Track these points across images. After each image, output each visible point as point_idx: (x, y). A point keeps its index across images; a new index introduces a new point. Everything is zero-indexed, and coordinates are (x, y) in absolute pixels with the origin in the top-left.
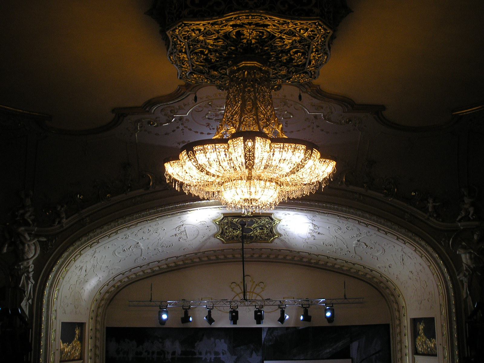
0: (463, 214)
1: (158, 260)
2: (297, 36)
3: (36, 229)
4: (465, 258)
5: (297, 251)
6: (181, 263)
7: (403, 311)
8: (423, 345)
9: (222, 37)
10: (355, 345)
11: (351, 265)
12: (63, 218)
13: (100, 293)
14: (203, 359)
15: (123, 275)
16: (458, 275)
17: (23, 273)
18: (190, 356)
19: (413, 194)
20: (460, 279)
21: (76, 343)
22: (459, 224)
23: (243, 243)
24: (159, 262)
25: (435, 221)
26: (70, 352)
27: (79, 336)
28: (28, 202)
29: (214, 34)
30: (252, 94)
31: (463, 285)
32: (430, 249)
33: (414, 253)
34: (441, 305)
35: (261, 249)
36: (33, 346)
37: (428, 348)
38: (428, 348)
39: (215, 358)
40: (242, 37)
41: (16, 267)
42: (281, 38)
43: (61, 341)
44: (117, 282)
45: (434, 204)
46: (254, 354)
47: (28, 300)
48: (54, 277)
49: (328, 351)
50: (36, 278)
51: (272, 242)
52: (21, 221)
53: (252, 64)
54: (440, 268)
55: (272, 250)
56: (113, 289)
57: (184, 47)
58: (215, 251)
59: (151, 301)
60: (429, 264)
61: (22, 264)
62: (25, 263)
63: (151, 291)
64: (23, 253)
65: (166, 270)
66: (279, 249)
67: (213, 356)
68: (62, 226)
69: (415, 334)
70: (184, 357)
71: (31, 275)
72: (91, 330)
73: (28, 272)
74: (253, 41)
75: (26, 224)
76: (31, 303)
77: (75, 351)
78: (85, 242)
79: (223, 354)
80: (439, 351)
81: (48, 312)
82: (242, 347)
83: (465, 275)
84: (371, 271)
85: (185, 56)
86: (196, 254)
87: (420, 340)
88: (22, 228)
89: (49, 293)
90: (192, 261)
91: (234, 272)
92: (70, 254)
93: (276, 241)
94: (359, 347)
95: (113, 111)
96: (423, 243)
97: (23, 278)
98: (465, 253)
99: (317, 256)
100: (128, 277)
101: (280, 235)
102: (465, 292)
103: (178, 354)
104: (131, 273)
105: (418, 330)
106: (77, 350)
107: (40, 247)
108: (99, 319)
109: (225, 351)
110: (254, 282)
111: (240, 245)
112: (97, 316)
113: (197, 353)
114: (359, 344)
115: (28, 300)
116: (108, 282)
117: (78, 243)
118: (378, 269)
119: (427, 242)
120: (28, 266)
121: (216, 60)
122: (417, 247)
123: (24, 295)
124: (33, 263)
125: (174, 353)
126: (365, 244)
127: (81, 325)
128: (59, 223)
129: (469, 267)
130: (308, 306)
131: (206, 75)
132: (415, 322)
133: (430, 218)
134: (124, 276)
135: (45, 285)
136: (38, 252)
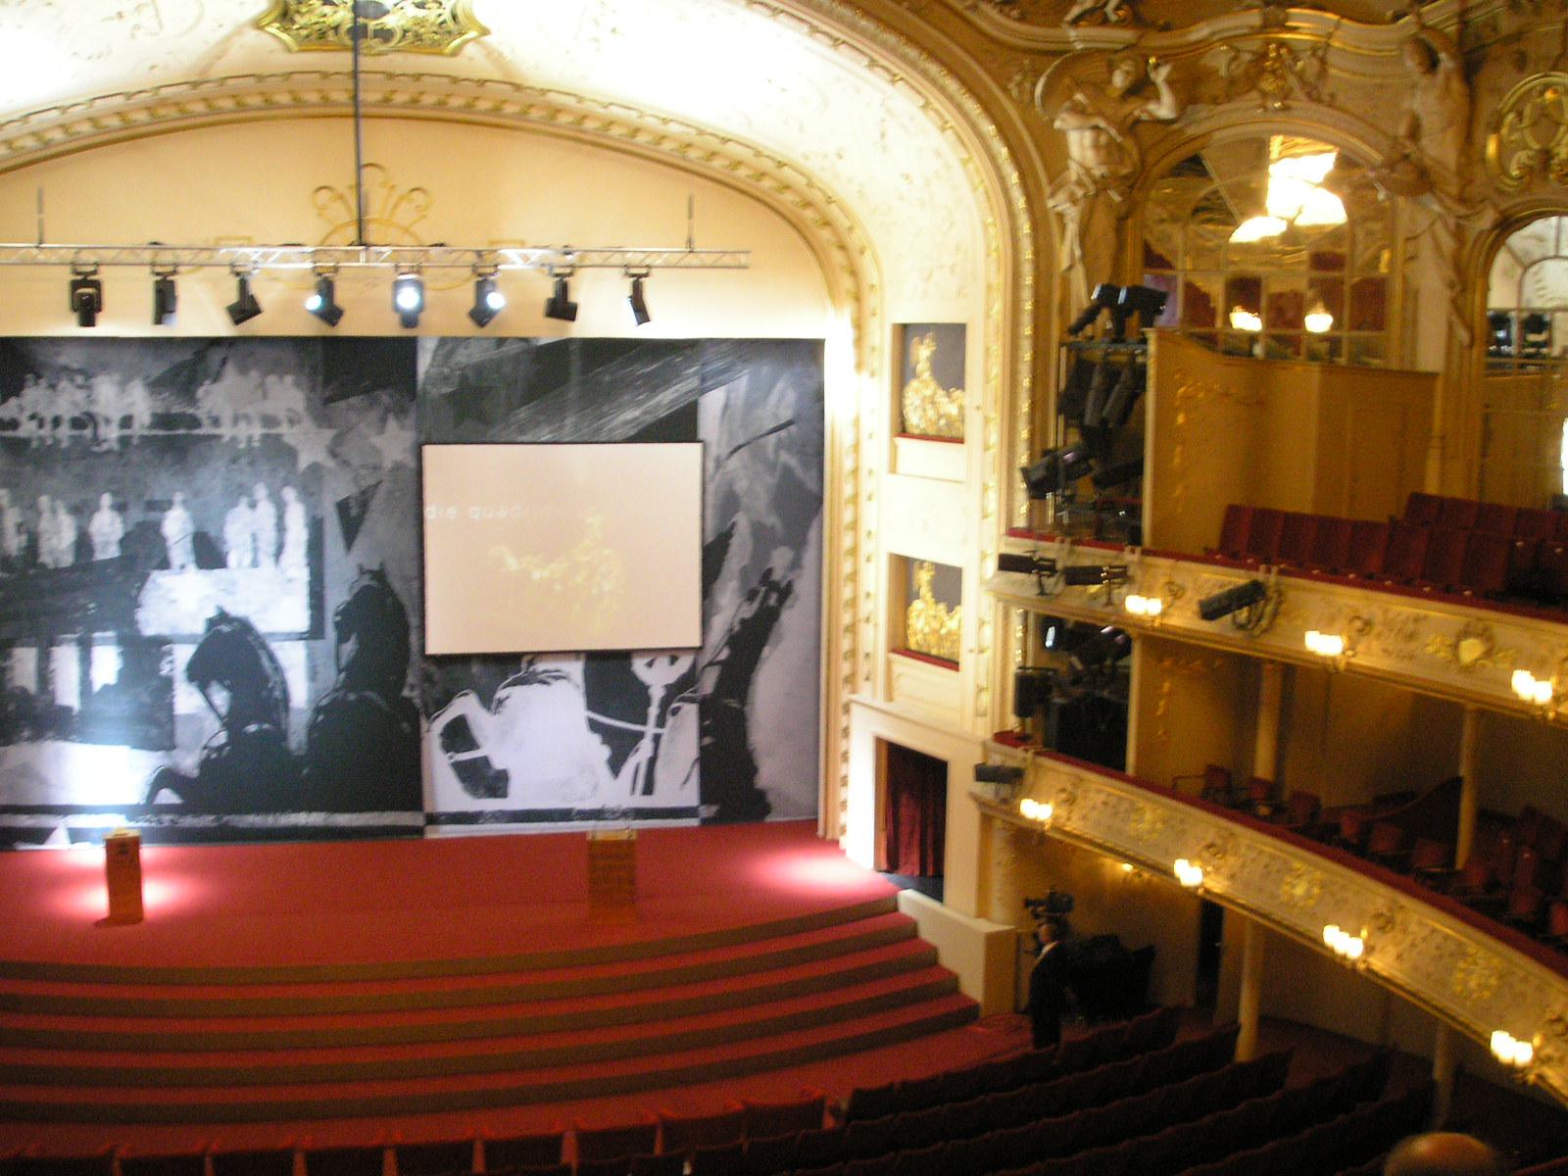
4: (1080, 146)
5: (539, 86)
6: (142, 117)
7: (871, 301)
8: (924, 410)
10: (712, 405)
11: (715, 144)
14: (226, 439)
16: (1053, 195)
18: (182, 432)
20: (1059, 209)
22: (1072, 33)
23: (355, 50)
24: (64, 109)
25: (994, 13)
31: (1063, 228)
32: (972, 107)
33: (920, 115)
34: (989, 287)
35: (418, 77)
37: (940, 417)
38: (940, 417)
39: (265, 437)
46: (392, 424)
49: (630, 414)
51: (455, 53)
54: (997, 169)
55: (455, 80)
58: (260, 78)
60: (965, 156)
63: (41, 211)
65: (91, 141)
66: (478, 81)
67: (257, 431)
69: (903, 373)
70: (161, 433)
79: (292, 422)
80: (973, 430)
82: (353, 400)
83: (1074, 201)
84: (781, 165)
86: (195, 85)
87: (917, 391)
90: (181, 111)
91: (327, 151)
93: (470, 50)
94: (726, 407)
96: (952, 85)
98: (1080, 128)
99: (605, 107)
101: (485, 32)
102: (1067, 250)
105: (913, 359)
109: (297, 413)
110: (393, 187)
111: (343, 61)
113: (206, 422)
114: (728, 399)
118: (801, 162)
119: (963, 82)
122: (932, 100)
125: (127, 422)
129: (1088, 171)
130: (568, 271)
132: (905, 333)
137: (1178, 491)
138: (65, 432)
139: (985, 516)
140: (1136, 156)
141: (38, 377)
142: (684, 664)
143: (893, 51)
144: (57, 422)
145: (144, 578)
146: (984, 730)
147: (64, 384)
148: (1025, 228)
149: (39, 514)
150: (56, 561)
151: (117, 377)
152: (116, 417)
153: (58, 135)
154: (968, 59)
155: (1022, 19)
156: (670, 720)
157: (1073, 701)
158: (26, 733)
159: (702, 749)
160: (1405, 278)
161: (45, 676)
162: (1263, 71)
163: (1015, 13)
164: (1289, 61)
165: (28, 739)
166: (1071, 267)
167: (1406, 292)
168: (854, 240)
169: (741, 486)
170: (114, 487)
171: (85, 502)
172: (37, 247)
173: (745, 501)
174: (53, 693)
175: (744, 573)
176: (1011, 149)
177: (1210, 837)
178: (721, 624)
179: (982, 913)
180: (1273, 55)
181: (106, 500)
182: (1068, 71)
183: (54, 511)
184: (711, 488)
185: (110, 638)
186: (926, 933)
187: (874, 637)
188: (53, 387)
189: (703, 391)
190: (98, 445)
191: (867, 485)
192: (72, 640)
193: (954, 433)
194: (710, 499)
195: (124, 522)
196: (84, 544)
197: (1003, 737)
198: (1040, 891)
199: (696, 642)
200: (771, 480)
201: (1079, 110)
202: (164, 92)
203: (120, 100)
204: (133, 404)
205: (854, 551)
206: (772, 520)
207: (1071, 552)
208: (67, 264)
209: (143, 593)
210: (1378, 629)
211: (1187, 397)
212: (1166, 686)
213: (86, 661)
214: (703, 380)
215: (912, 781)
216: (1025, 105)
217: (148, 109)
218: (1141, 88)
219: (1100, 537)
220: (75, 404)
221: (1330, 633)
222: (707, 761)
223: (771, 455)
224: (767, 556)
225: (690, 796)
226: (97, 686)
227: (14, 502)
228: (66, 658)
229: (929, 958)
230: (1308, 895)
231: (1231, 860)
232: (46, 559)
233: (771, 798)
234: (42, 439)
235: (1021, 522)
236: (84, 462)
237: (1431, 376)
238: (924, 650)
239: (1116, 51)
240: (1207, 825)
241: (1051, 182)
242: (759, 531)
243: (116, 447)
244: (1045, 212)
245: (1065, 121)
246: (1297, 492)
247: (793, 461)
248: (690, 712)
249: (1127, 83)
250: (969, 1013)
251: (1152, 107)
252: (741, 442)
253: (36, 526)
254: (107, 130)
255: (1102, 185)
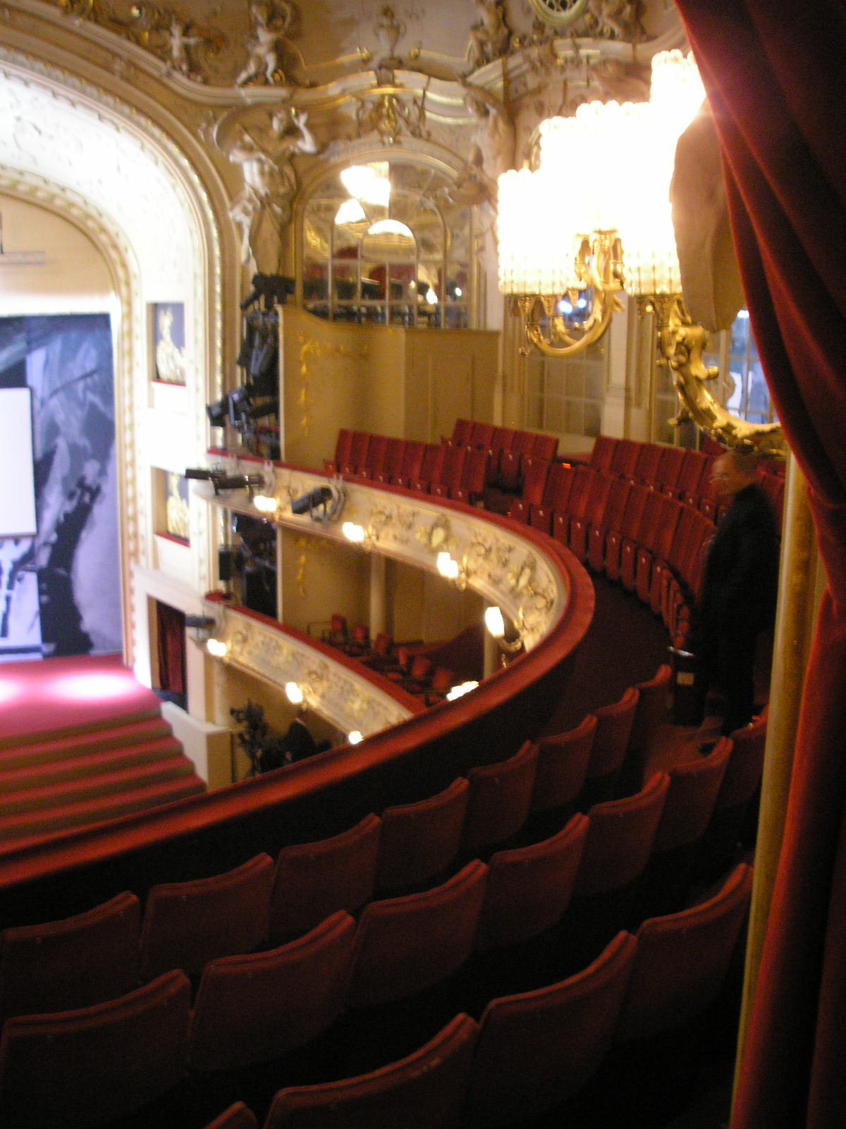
0: (252, 68)
7: (134, 285)
8: (168, 363)
10: (36, 362)
11: (17, 177)
16: (232, 209)
19: (135, 12)
22: (243, 92)
25: (184, 80)
34: (195, 276)
37: (176, 367)
45: (185, 40)
60: (173, 181)
69: (155, 337)
80: (189, 379)
83: (246, 212)
84: (63, 190)
102: (243, 249)
105: (160, 327)
126: (36, 128)
129: (256, 192)
132: (155, 309)
133: (177, 75)
137: (304, 422)
139: (198, 438)
140: (293, 180)
142: (25, 546)
143: (114, 109)
146: (204, 588)
148: (215, 233)
154: (168, 114)
155: (206, 82)
156: (17, 584)
157: (249, 571)
159: (42, 606)
160: (479, 265)
162: (380, 117)
163: (199, 78)
164: (398, 109)
166: (248, 260)
167: (479, 273)
168: (122, 242)
169: (60, 418)
173: (63, 428)
175: (65, 481)
176: (200, 176)
177: (315, 667)
178: (50, 517)
179: (210, 718)
180: (387, 104)
182: (236, 121)
184: (38, 421)
186: (178, 734)
187: (146, 524)
189: (29, 350)
191: (138, 416)
193: (180, 379)
194: (38, 427)
197: (212, 597)
198: (241, 704)
199: (31, 528)
200: (80, 414)
201: (248, 149)
205: (133, 463)
206: (84, 442)
207: (238, 464)
210: (394, 520)
211: (307, 353)
212: (303, 559)
214: (29, 343)
215: (169, 624)
216: (207, 146)
218: (291, 131)
219: (257, 456)
221: (373, 523)
222: (46, 614)
223: (80, 395)
224: (81, 467)
225: (35, 638)
229: (178, 752)
230: (361, 709)
231: (325, 684)
233: (93, 638)
235: (220, 443)
237: (494, 335)
238: (177, 532)
239: (275, 104)
240: (314, 658)
241: (231, 198)
242: (75, 450)
244: (227, 221)
245: (236, 156)
246: (392, 422)
247: (96, 399)
248: (31, 580)
249: (281, 127)
250: (202, 786)
251: (300, 144)
252: (58, 385)
255: (265, 202)
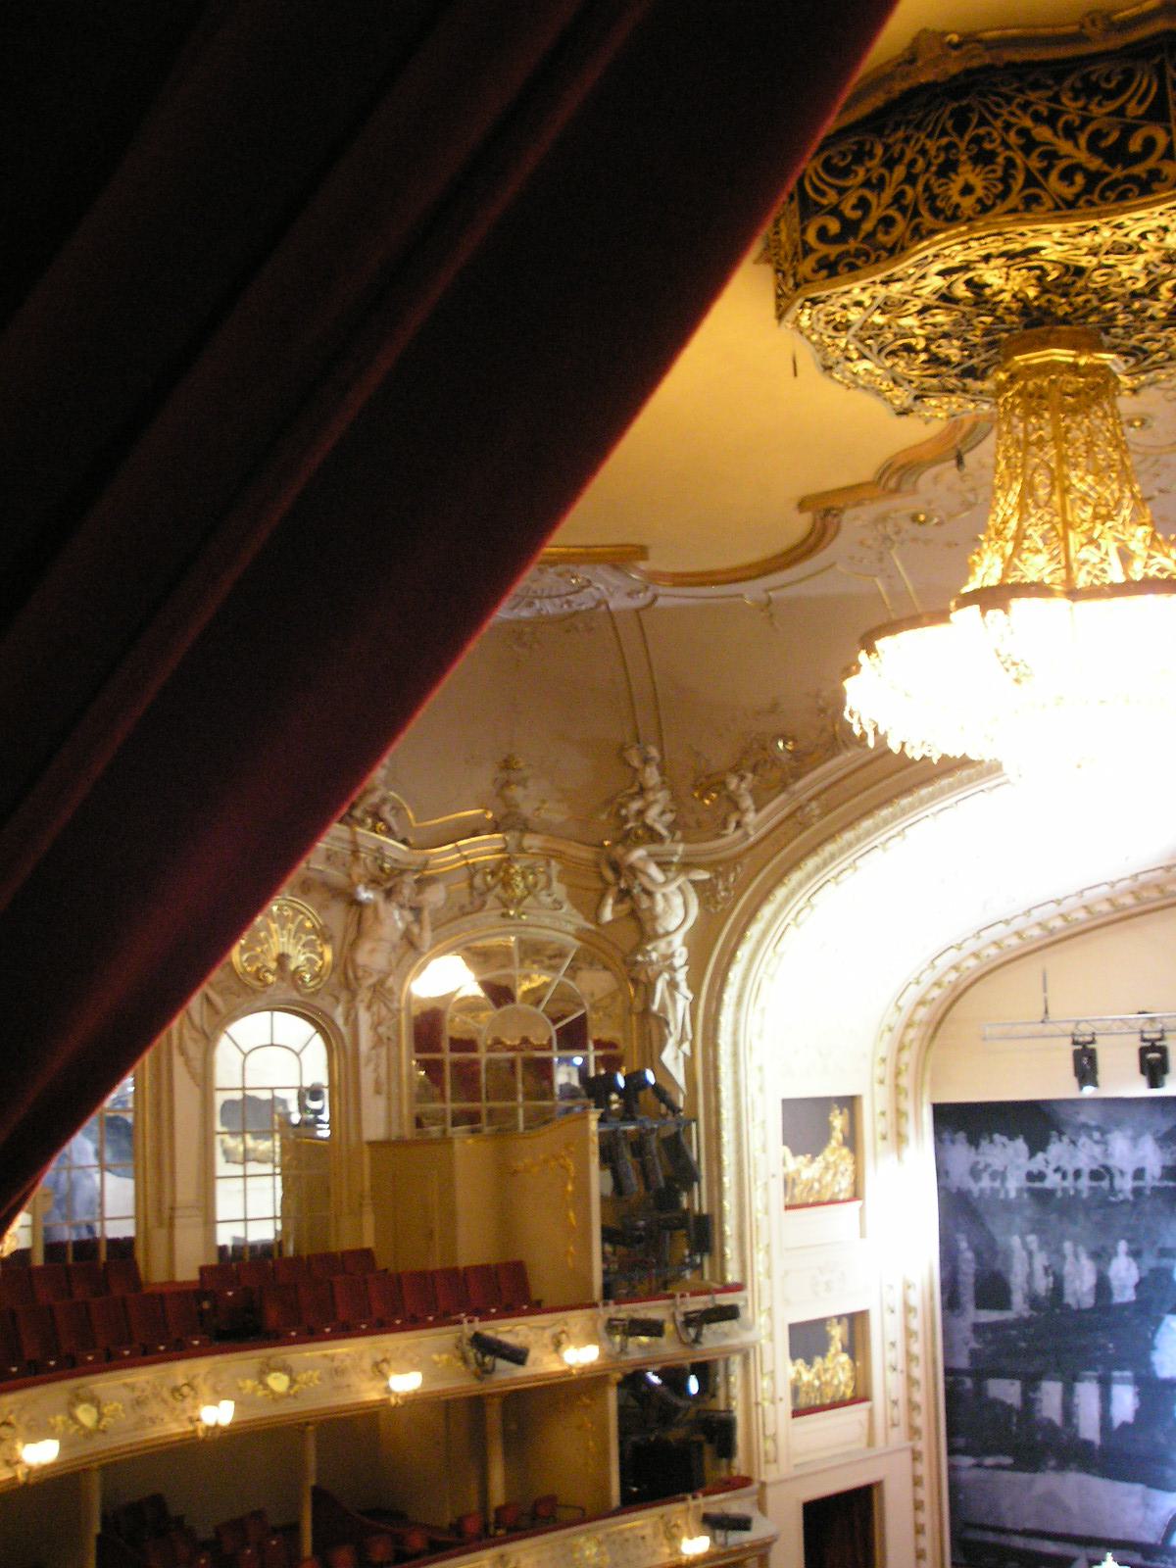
1: (1053, 898)
2: (1146, 251)
3: (680, 848)
6: (1128, 900)
9: (937, 303)
12: (747, 810)
13: (899, 1009)
15: (959, 949)
17: (660, 973)
21: (835, 1152)
24: (1058, 902)
26: (819, 1181)
27: (847, 1134)
28: (652, 776)
29: (906, 301)
30: (1051, 452)
36: (703, 1166)
40: (988, 292)
41: (640, 958)
42: (1101, 266)
43: (786, 1150)
44: (945, 974)
47: (680, 1042)
48: (745, 978)
50: (694, 986)
52: (640, 832)
53: (1047, 355)
56: (936, 992)
57: (851, 347)
59: (1043, 1022)
61: (654, 949)
62: (662, 945)
63: (1045, 991)
64: (655, 918)
68: (746, 835)
71: (681, 976)
72: (883, 1114)
73: (672, 969)
74: (1032, 293)
75: (653, 837)
76: (688, 1053)
77: (835, 1175)
78: (818, 869)
81: (736, 1072)
85: (866, 364)
88: (638, 854)
89: (736, 1022)
92: (782, 907)
95: (803, 505)
97: (661, 985)
100: (976, 955)
103: (1153, 1178)
104: (980, 944)
106: (843, 1174)
107: (699, 897)
108: (906, 1081)
112: (898, 1074)
115: (680, 1042)
116: (916, 975)
117: (796, 877)
120: (670, 951)
121: (963, 356)
123: (667, 1031)
124: (685, 944)
125: (1139, 1174)
127: (850, 1103)
128: (739, 825)
131: (959, 393)
134: (965, 952)
135: (719, 1000)
136: (694, 910)
138: (1085, 1182)
141: (1061, 1133)
144: (1077, 1174)
145: (1158, 1322)
147: (1083, 1140)
149: (1064, 1257)
150: (1078, 1302)
151: (1129, 1133)
152: (1130, 1170)
153: (1058, 923)
158: (1052, 1463)
161: (1068, 1410)
165: (1054, 1469)
170: (1128, 1235)
171: (1103, 1249)
172: (1043, 1022)
174: (1076, 1427)
181: (1123, 1246)
183: (1076, 1256)
185: (1127, 1378)
188: (1073, 1143)
190: (1115, 1195)
192: (1089, 1378)
195: (1139, 1268)
196: (1103, 1287)
202: (1142, 878)
203: (1105, 889)
204: (1144, 1158)
208: (1066, 1035)
209: (1158, 1336)
213: (1106, 1399)
217: (1133, 893)
220: (1093, 1158)
226: (1117, 1421)
227: (1044, 1244)
228: (1087, 1393)
232: (1069, 1299)
234: (1065, 1190)
236: (1102, 1211)
243: (1131, 1197)
253: (1062, 1268)
254: (1101, 914)
